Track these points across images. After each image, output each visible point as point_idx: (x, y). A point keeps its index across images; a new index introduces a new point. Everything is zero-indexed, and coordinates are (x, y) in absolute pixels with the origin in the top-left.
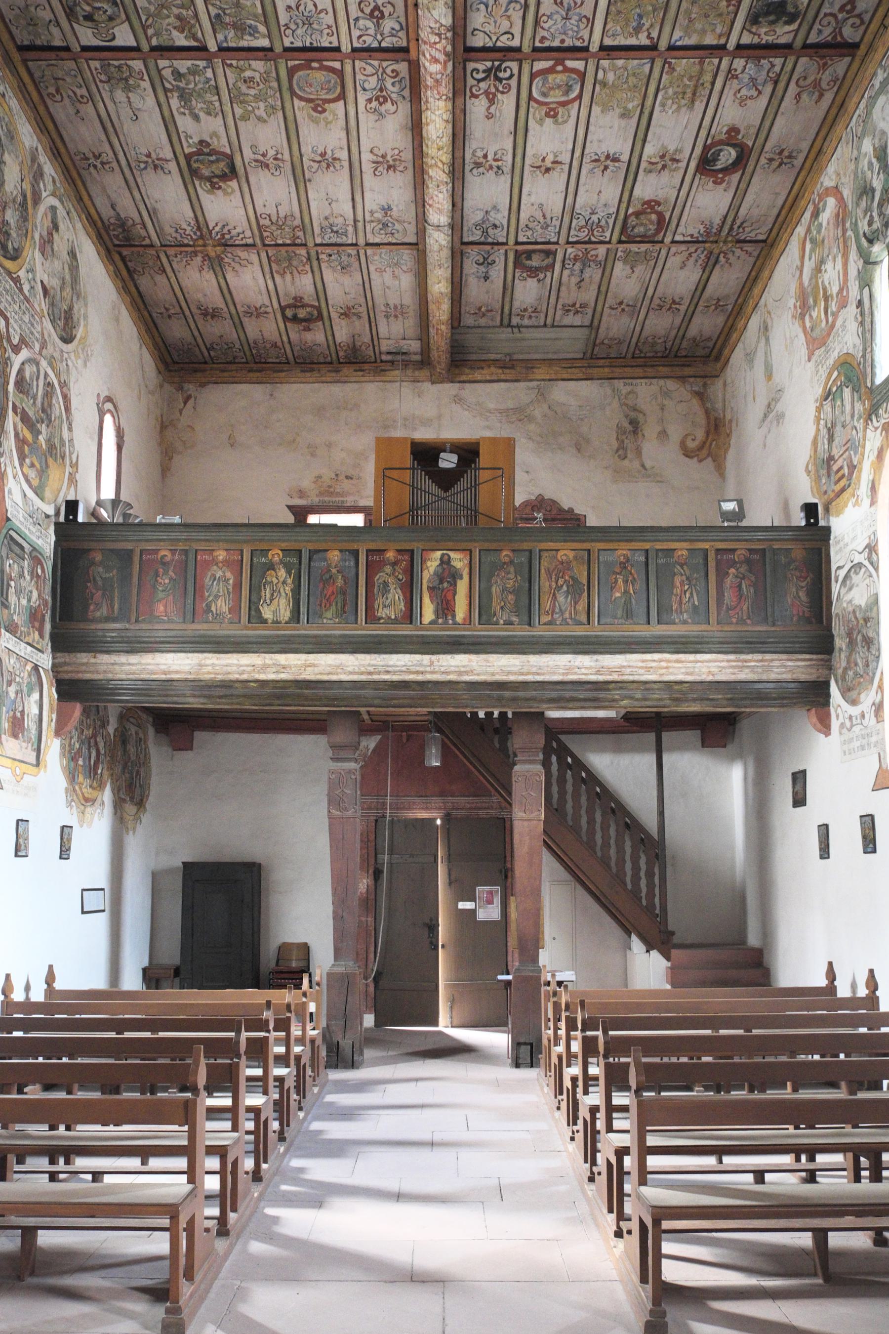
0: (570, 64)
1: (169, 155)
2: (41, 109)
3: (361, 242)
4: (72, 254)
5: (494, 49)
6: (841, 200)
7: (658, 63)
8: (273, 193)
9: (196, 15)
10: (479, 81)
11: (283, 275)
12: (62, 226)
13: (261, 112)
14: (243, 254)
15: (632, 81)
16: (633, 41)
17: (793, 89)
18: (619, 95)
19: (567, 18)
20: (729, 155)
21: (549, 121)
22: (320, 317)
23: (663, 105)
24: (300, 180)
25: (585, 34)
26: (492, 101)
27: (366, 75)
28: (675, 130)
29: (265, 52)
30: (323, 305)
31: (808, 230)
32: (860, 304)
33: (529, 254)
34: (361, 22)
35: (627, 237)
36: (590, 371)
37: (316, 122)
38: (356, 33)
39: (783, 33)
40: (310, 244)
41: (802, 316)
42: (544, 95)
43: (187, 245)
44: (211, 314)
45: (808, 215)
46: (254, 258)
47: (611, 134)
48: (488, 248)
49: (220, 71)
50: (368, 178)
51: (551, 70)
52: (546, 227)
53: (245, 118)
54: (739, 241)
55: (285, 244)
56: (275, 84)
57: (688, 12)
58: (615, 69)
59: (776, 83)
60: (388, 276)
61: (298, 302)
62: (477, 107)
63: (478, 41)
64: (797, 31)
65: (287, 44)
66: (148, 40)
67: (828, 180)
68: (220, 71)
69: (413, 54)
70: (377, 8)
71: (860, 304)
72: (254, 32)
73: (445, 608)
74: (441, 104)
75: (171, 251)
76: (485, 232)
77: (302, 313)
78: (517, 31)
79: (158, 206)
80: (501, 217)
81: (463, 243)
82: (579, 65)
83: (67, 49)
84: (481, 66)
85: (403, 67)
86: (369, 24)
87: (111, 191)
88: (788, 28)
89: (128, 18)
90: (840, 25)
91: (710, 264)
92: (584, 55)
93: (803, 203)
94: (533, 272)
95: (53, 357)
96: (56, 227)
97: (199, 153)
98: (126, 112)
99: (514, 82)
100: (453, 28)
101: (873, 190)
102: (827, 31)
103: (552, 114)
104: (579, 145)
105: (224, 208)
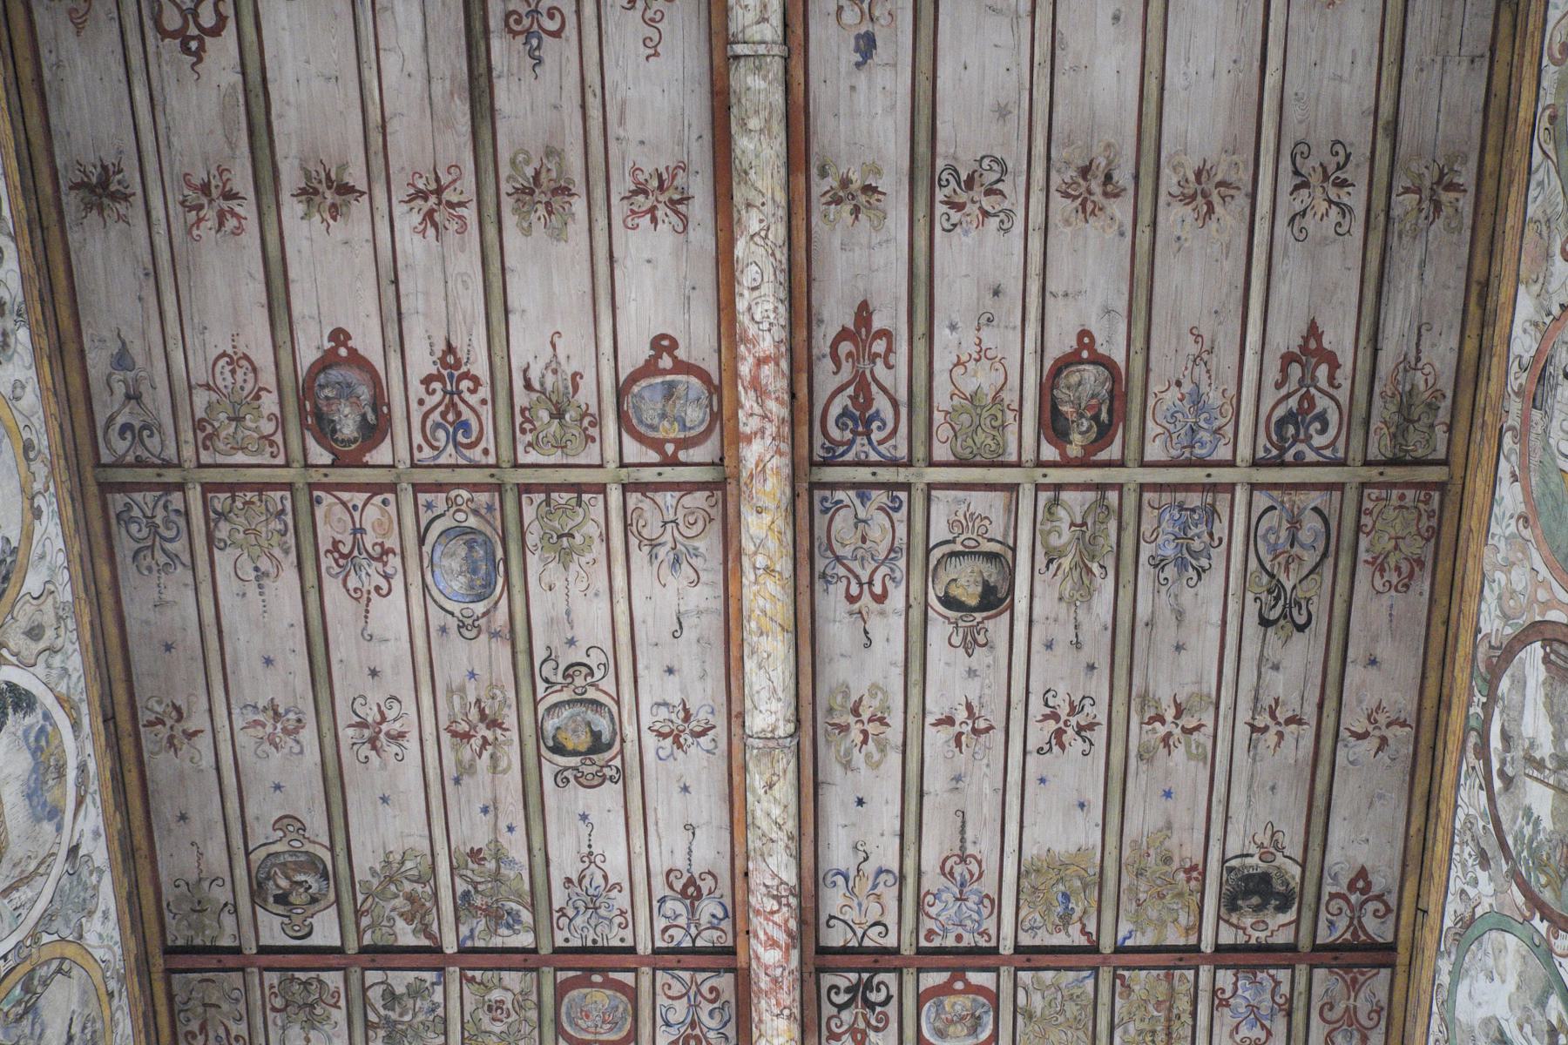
5: (860, 951)
7: (1105, 975)
9: (435, 894)
10: (841, 1007)
15: (1071, 1009)
16: (1059, 939)
19: (961, 899)
25: (990, 925)
29: (526, 960)
34: (669, 904)
38: (660, 923)
39: (1277, 927)
49: (454, 989)
51: (945, 990)
56: (533, 1015)
57: (1134, 890)
58: (1041, 988)
59: (1289, 1014)
63: (836, 937)
64: (1298, 921)
65: (560, 943)
66: (360, 938)
68: (454, 989)
70: (691, 881)
72: (513, 921)
78: (891, 919)
84: (842, 981)
86: (680, 908)
88: (1284, 918)
90: (1356, 912)
92: (990, 961)
99: (892, 1011)
102: (1342, 923)
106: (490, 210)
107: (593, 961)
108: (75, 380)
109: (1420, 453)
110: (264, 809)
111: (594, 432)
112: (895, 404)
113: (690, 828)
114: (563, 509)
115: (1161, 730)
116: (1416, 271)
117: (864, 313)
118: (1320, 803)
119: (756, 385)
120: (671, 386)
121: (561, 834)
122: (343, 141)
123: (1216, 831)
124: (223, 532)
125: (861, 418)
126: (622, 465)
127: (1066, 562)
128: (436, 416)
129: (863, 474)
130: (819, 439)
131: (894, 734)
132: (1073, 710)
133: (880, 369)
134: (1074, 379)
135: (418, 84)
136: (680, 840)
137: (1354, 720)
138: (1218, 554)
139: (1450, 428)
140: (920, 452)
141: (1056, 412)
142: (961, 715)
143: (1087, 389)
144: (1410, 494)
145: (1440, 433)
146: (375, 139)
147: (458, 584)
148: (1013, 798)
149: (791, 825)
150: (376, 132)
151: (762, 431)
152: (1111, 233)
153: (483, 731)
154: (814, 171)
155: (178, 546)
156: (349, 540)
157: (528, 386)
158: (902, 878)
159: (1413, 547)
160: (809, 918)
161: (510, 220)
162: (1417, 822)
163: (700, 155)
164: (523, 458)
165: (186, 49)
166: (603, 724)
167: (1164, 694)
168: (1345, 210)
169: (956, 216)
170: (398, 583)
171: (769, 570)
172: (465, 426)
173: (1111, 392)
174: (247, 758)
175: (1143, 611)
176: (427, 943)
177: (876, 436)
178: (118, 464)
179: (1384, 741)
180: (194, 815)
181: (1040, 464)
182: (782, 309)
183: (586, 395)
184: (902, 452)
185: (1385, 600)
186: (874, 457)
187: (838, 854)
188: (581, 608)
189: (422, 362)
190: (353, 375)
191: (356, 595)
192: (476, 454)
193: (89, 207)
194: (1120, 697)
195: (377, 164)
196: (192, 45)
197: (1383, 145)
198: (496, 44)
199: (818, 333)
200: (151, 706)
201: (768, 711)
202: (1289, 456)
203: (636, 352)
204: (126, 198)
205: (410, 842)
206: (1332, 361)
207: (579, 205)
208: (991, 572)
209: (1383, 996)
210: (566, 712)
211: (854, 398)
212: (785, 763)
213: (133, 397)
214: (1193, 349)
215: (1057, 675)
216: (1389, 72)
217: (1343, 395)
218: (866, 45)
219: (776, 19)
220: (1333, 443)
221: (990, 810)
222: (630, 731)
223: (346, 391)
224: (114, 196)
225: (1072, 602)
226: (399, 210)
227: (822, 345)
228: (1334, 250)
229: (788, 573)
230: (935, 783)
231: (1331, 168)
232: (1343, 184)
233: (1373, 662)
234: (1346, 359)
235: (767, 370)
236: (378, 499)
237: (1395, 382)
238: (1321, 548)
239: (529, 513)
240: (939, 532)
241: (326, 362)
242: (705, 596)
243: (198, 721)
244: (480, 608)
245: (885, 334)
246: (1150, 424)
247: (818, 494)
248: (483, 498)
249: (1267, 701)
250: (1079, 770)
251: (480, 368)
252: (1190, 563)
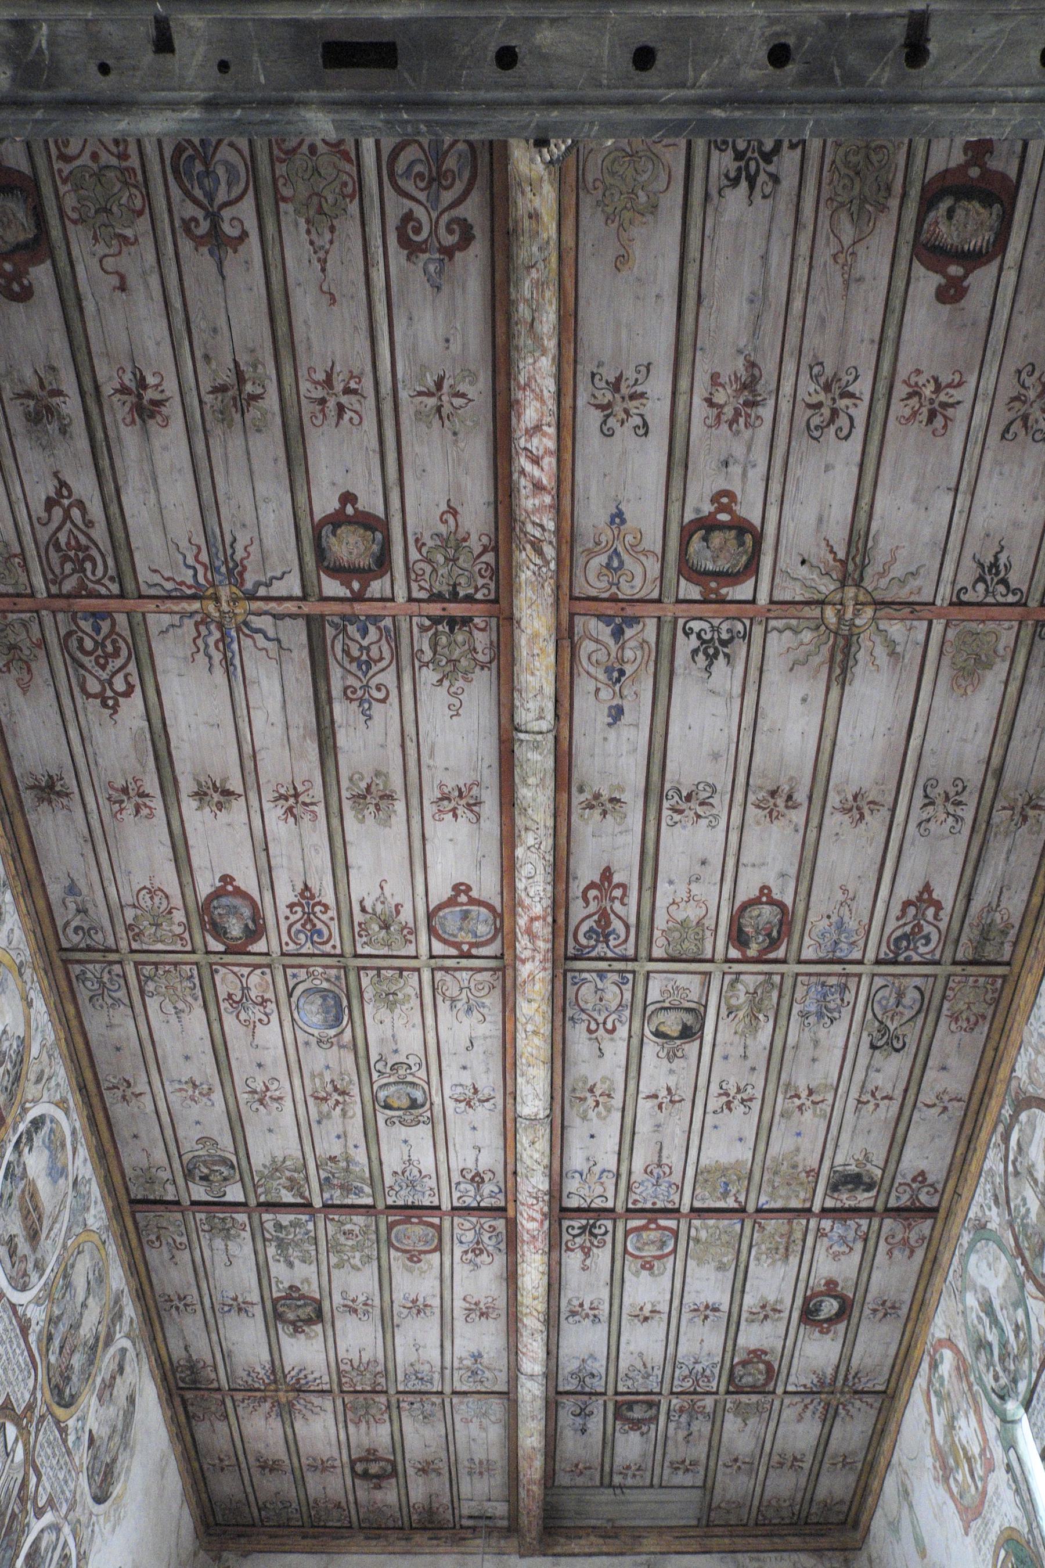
0: (662, 1222)
1: (255, 1297)
2: (137, 1254)
3: (448, 1390)
4: (131, 1400)
5: (589, 1210)
6: (957, 1352)
7: (748, 1224)
8: (358, 1339)
9: (307, 1178)
11: (357, 1424)
12: (128, 1369)
13: (356, 1261)
14: (316, 1400)
15: (725, 1238)
17: (883, 1247)
19: (657, 1184)
20: (830, 1307)
21: (645, 1273)
22: (394, 1473)
23: (758, 1259)
24: (388, 1324)
25: (676, 1198)
27: (465, 1229)
28: (772, 1281)
30: (399, 1459)
31: (930, 1382)
32: (1009, 1468)
33: (630, 1405)
34: (462, 1187)
35: (735, 1388)
36: (707, 1541)
37: (410, 1271)
39: (864, 1199)
40: (392, 1391)
41: (946, 1480)
42: (638, 1249)
43: (258, 1390)
44: (269, 1466)
45: (925, 1365)
46: (328, 1405)
48: (585, 1398)
49: (321, 1224)
50: (459, 1324)
51: (645, 1228)
52: (647, 1376)
53: (340, 1266)
54: (856, 1392)
55: (364, 1392)
57: (771, 1182)
58: (707, 1228)
59: (866, 1240)
60: (474, 1427)
61: (371, 1456)
62: (573, 1260)
63: (573, 1203)
65: (390, 1202)
66: (257, 1197)
67: (938, 1328)
68: (321, 1224)
69: (511, 1213)
70: (478, 1174)
71: (1009, 1468)
72: (359, 1192)
74: (538, 1257)
75: (239, 1396)
76: (582, 1381)
77: (374, 1469)
78: (610, 1193)
79: (233, 1348)
80: (599, 1366)
81: (558, 1393)
82: (672, 1224)
83: (177, 1203)
84: (576, 1224)
85: (500, 1224)
86: (470, 1187)
87: (189, 1337)
88: (866, 1195)
89: (242, 1179)
91: (829, 1417)
93: (917, 1354)
94: (636, 1425)
95: (79, 1521)
96: (121, 1369)
98: (220, 1258)
99: (608, 1238)
100: (550, 1192)
101: (990, 1345)
102: (906, 1197)
103: (648, 1266)
104: (678, 1294)
105: (304, 1353)
106: (334, 808)
107: (411, 1211)
108: (41, 904)
109: (992, 957)
110: (189, 1135)
111: (412, 938)
112: (627, 927)
114: (390, 980)
115: (797, 1102)
116: (1004, 856)
117: (607, 874)
119: (529, 932)
120: (467, 912)
121: (390, 1150)
122: (226, 766)
123: (829, 1153)
124: (150, 986)
125: (602, 931)
126: (432, 957)
127: (741, 1014)
128: (298, 926)
129: (603, 965)
130: (571, 943)
132: (739, 1091)
133: (617, 906)
134: (755, 913)
135: (279, 730)
137: (927, 1096)
138: (846, 1012)
139: (1015, 944)
140: (643, 953)
141: (740, 930)
142: (663, 1093)
143: (762, 920)
144: (982, 980)
145: (1008, 948)
146: (249, 764)
147: (317, 1019)
150: (249, 761)
151: (533, 958)
152: (789, 830)
153: (335, 1096)
154: (574, 790)
155: (121, 994)
156: (239, 994)
157: (363, 910)
158: (618, 1175)
159: (979, 1008)
160: (555, 1192)
161: (349, 815)
163: (490, 778)
164: (360, 951)
165: (104, 705)
166: (418, 1095)
167: (802, 1084)
168: (957, 819)
169: (677, 817)
170: (274, 1018)
171: (535, 1033)
172: (320, 933)
173: (781, 922)
174: (176, 1107)
175: (791, 1040)
176: (300, 1200)
177: (612, 943)
178: (74, 949)
179: (945, 1109)
180: (143, 1135)
181: (727, 961)
182: (549, 888)
183: (406, 915)
184: (631, 952)
185: (957, 1036)
186: (610, 954)
187: (576, 1159)
188: (402, 1034)
189: (286, 894)
190: (237, 902)
191: (246, 1023)
192: (327, 948)
193: (41, 800)
194: (771, 1087)
195: (251, 779)
196: (109, 702)
197: (991, 783)
198: (337, 708)
199: (573, 885)
200: (108, 1076)
201: (533, 1100)
202: (901, 958)
203: (441, 891)
204: (67, 795)
205: (288, 1152)
206: (938, 906)
207: (400, 806)
208: (689, 1019)
209: (927, 1232)
210: (393, 1089)
211: (598, 922)
213: (82, 911)
214: (839, 896)
215: (730, 1074)
216: (1001, 738)
217: (943, 925)
218: (617, 713)
219: (550, 716)
220: (933, 951)
221: (680, 1140)
222: (437, 1100)
223: (234, 911)
224: (59, 794)
225: (743, 1034)
226: (266, 806)
227: (577, 888)
228: (948, 843)
229: (548, 1033)
230: (644, 1127)
231: (952, 794)
232: (960, 803)
233: (944, 1068)
234: (948, 905)
235: (537, 925)
236: (258, 971)
237: (980, 917)
238: (917, 1007)
239: (365, 982)
240: (654, 995)
241: (217, 894)
242: (488, 1029)
243: (142, 1087)
244: (332, 1032)
245: (623, 886)
246: (806, 938)
247: (569, 975)
248: (333, 972)
249: (870, 1087)
250: (742, 1122)
251: (329, 899)
252: (825, 1014)
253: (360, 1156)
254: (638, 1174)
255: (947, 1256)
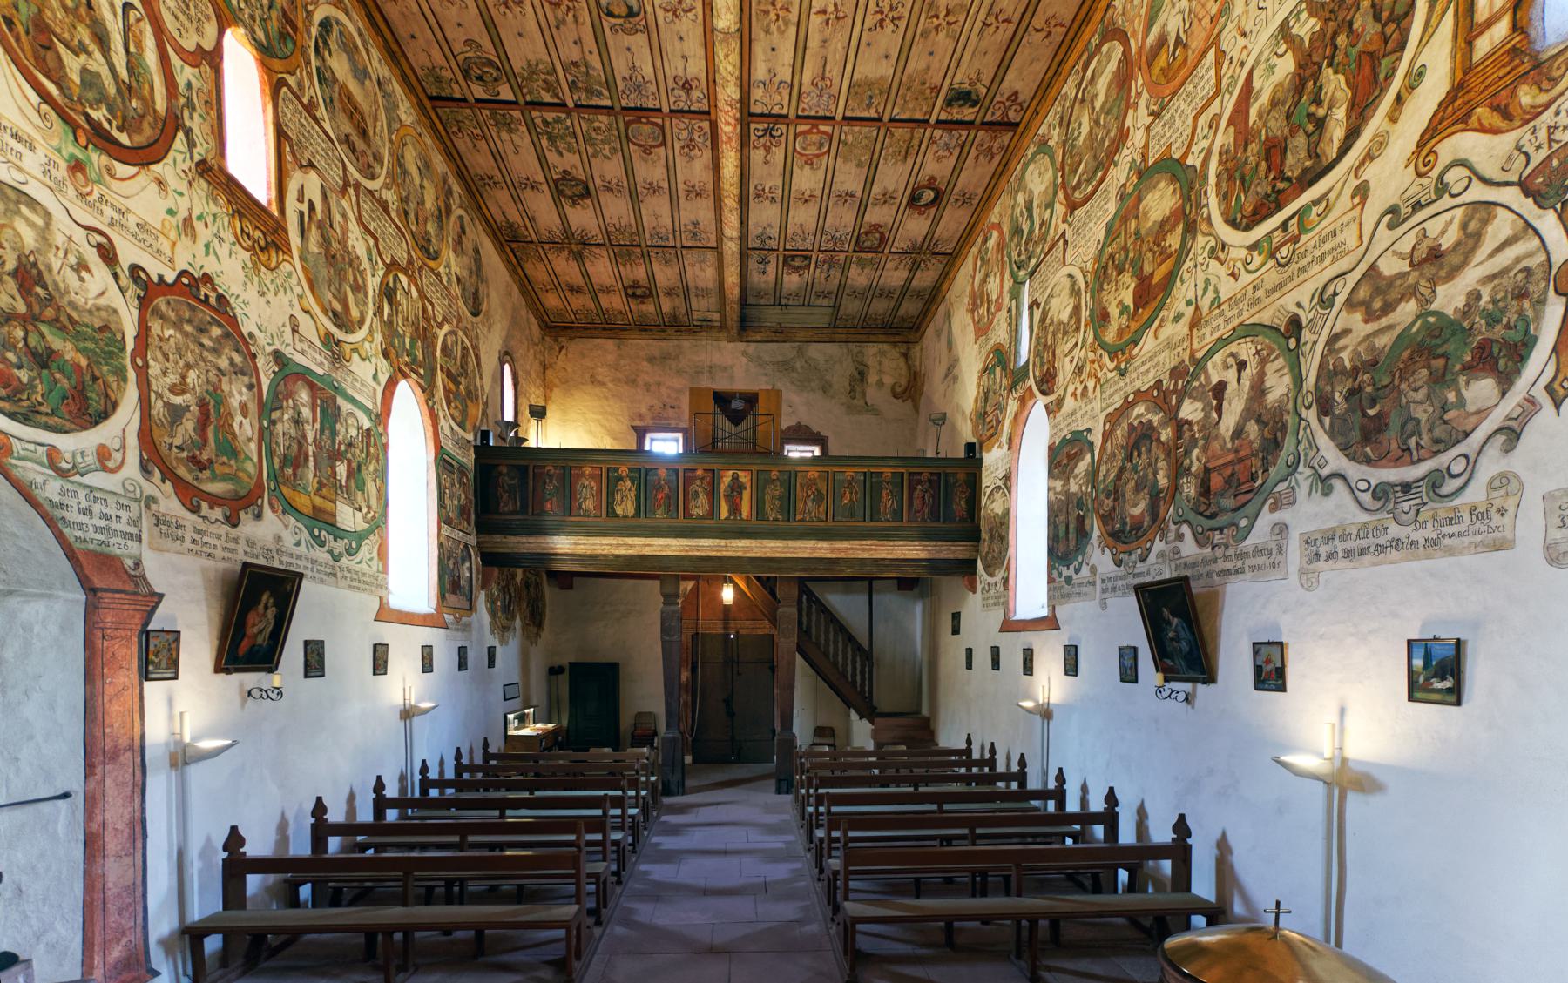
0: (822, 128)
1: (542, 179)
5: (770, 115)
8: (617, 209)
15: (865, 142)
16: (865, 114)
17: (973, 152)
18: (856, 151)
19: (820, 96)
26: (768, 152)
27: (680, 129)
28: (893, 177)
34: (676, 92)
38: (672, 99)
39: (968, 113)
47: (849, 179)
49: (576, 122)
53: (595, 155)
57: (904, 96)
58: (853, 133)
63: (757, 109)
68: (576, 122)
69: (713, 117)
73: (735, 509)
78: (785, 102)
82: (828, 129)
84: (761, 127)
85: (706, 125)
86: (682, 93)
87: (500, 202)
90: (1007, 109)
97: (563, 179)
98: (510, 148)
99: (783, 139)
100: (741, 101)
102: (998, 113)
105: (582, 218)
113: (685, 57)
118: (1006, 62)
131: (793, 17)
136: (680, 64)
142: (831, 8)
148: (852, 51)
149: (737, 73)
158: (792, 86)
160: (745, 100)
162: (1050, 74)
176: (556, 101)
187: (760, 72)
212: (735, 45)
221: (839, 56)
230: (814, 43)
250: (889, 40)
253: (595, 61)
254: (806, 88)
255: (1015, 162)
